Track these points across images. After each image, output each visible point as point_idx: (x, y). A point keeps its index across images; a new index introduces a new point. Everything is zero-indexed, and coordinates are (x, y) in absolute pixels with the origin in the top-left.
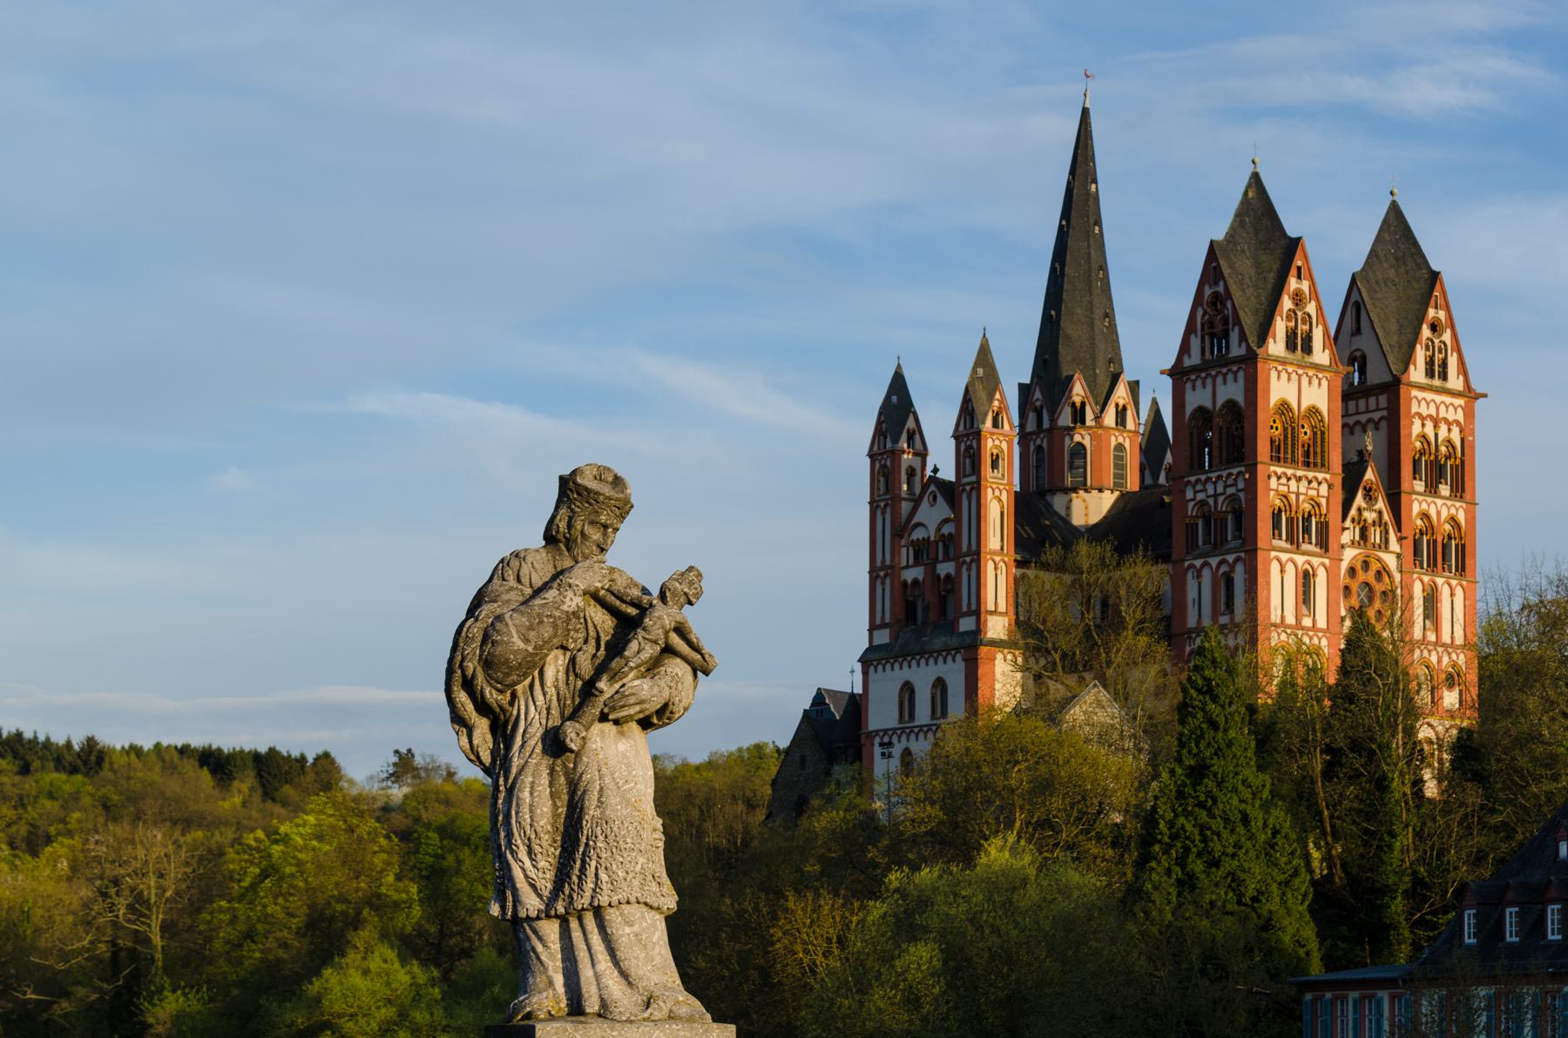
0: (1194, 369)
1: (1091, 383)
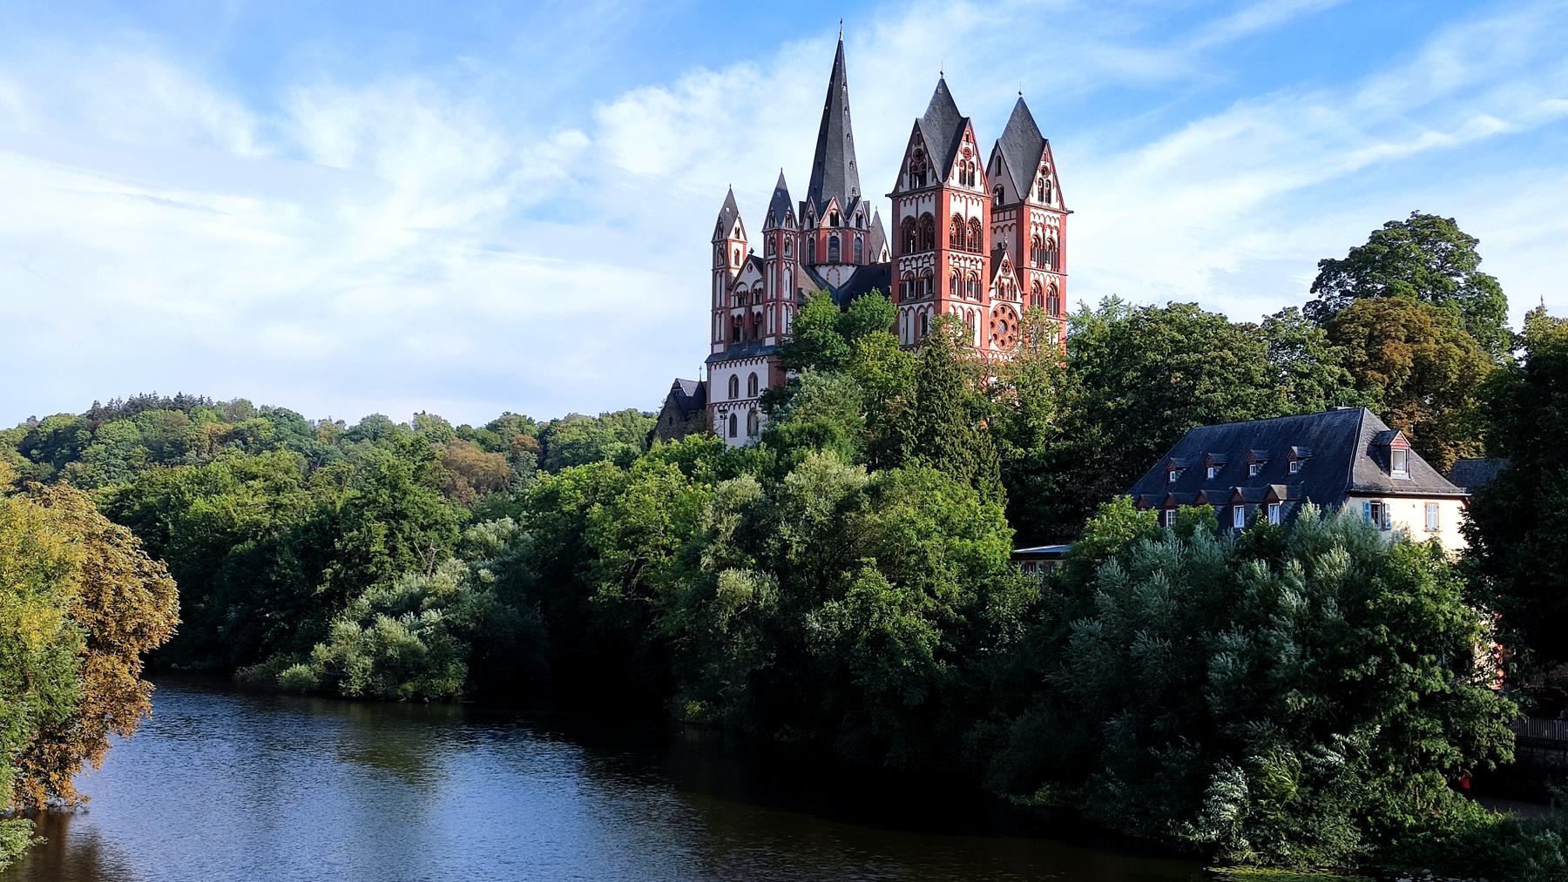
0: (905, 194)
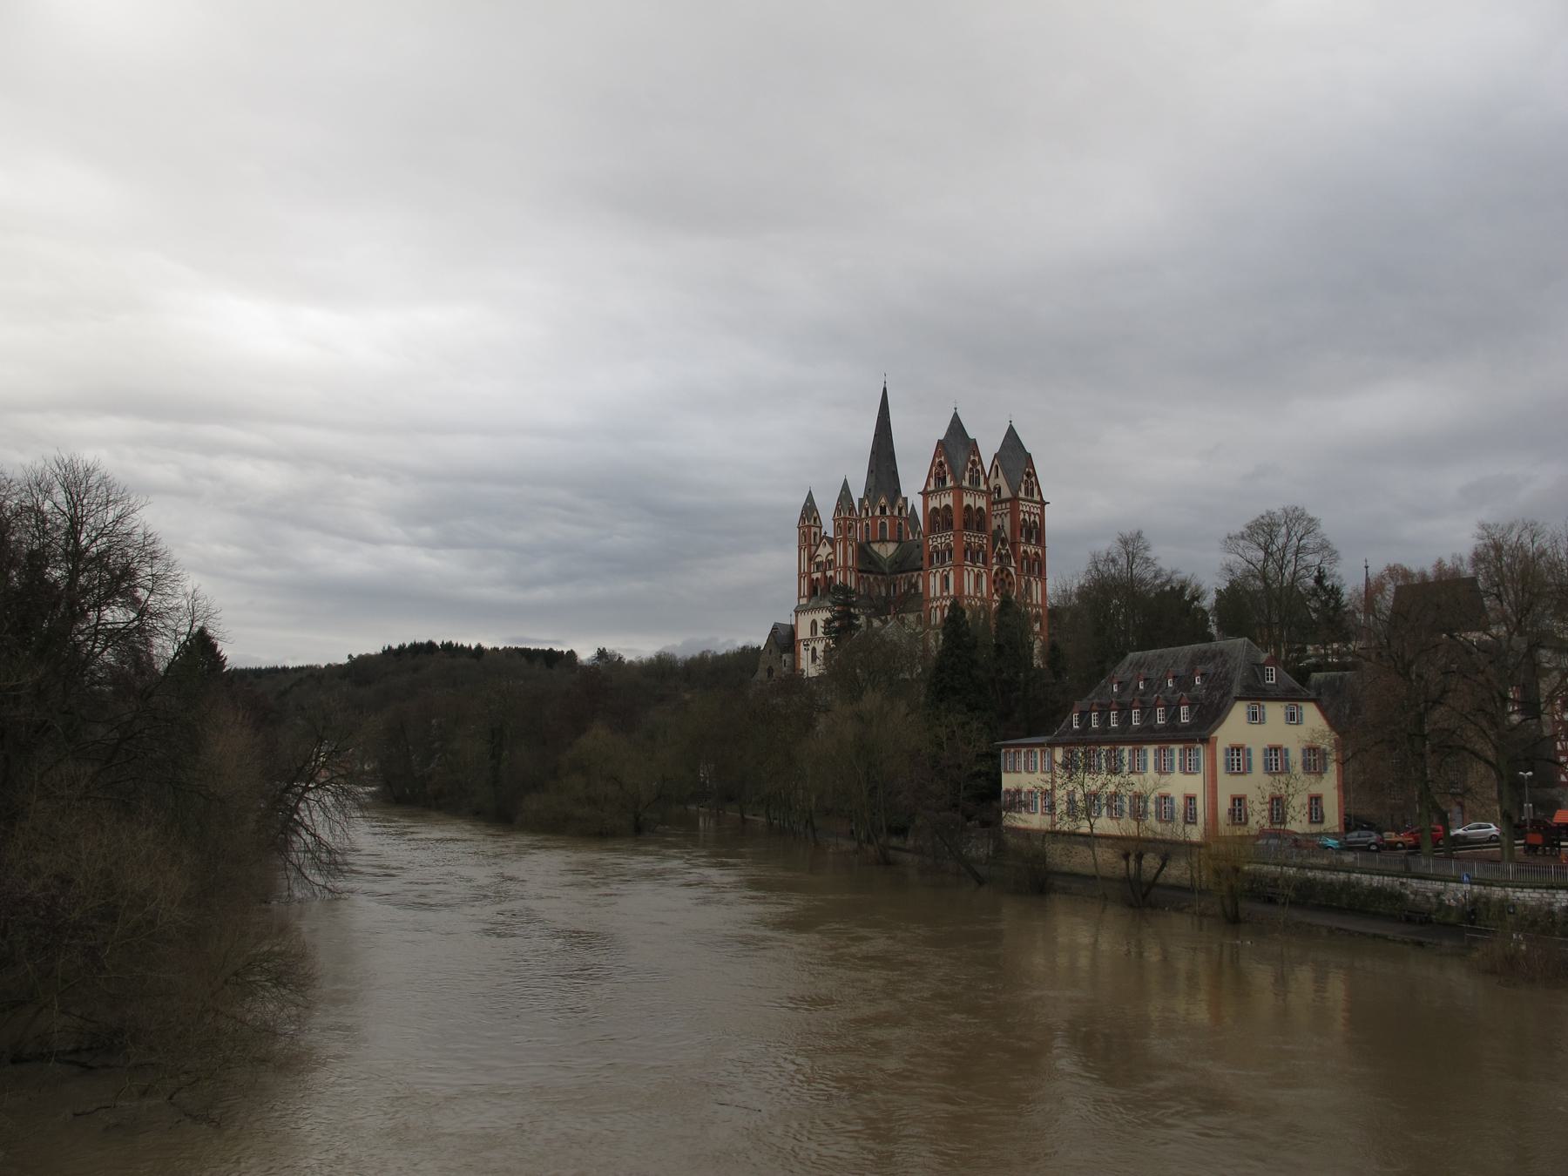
1: (887, 498)
